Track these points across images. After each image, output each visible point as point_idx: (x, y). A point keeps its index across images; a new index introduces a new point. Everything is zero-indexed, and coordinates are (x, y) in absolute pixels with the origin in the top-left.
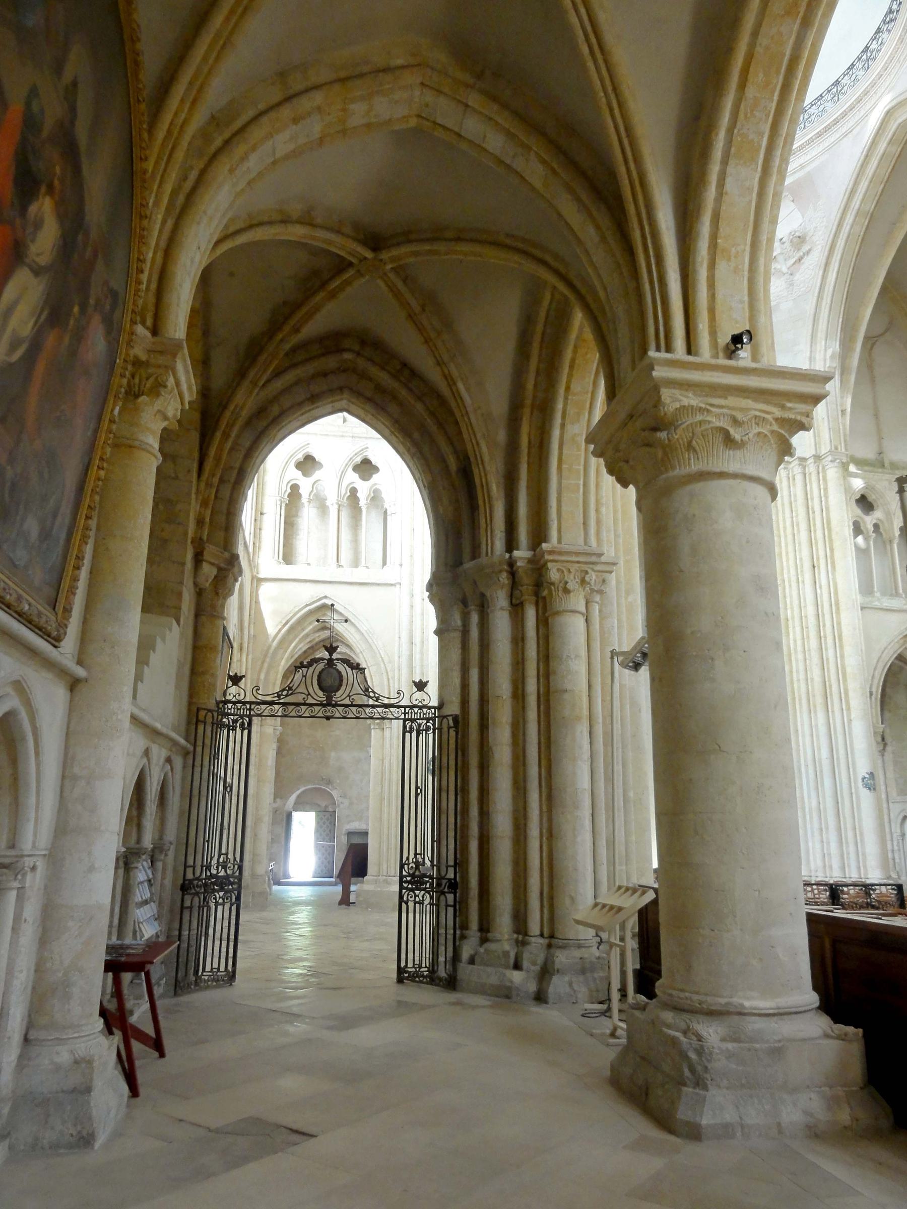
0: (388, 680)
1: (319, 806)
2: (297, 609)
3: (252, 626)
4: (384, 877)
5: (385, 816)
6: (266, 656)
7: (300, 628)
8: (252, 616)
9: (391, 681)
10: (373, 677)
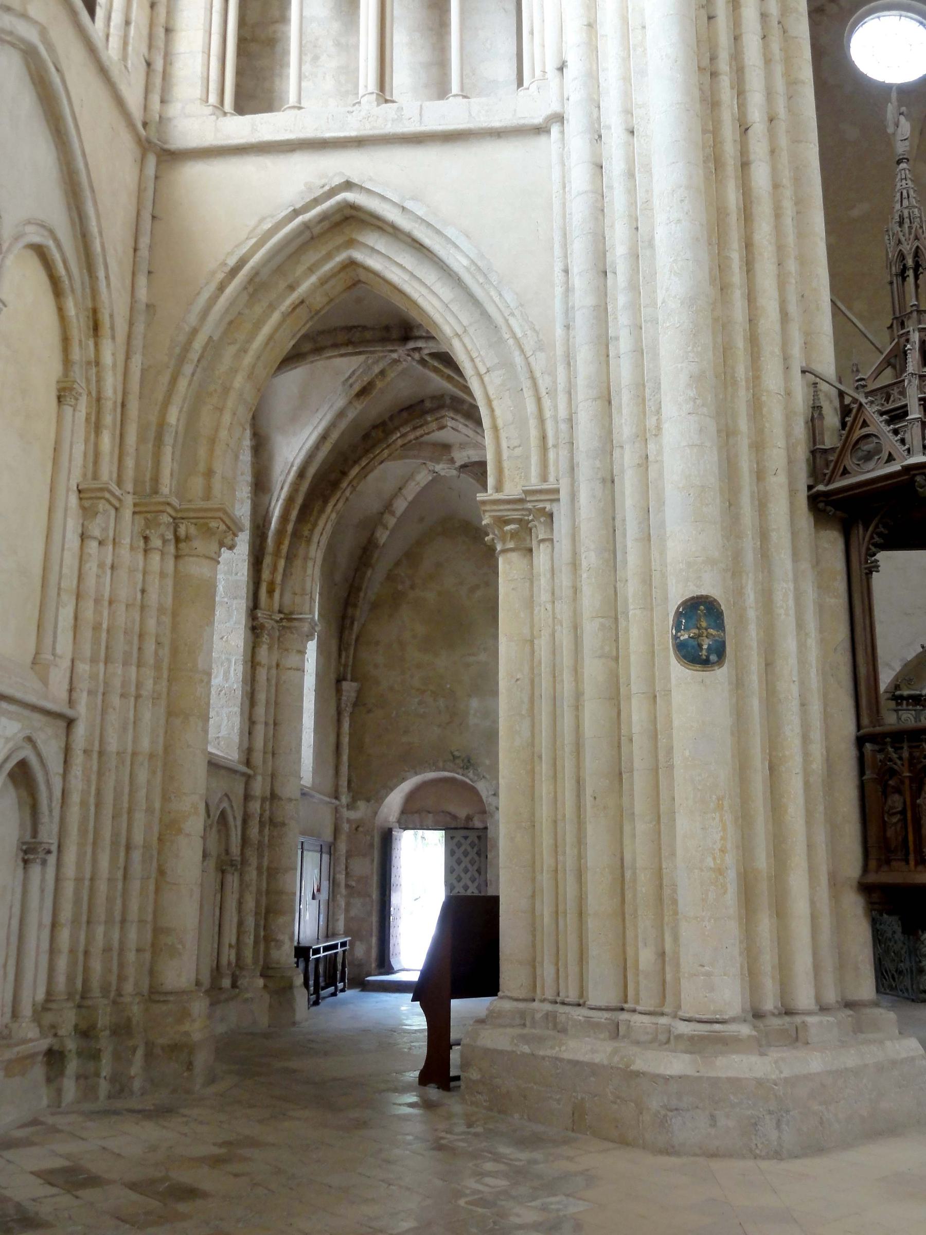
0: (539, 400)
1: (455, 817)
2: (267, 225)
3: (142, 281)
4: (548, 1007)
5: (544, 812)
6: (182, 359)
7: (282, 285)
8: (144, 252)
9: (547, 403)
10: (495, 404)
